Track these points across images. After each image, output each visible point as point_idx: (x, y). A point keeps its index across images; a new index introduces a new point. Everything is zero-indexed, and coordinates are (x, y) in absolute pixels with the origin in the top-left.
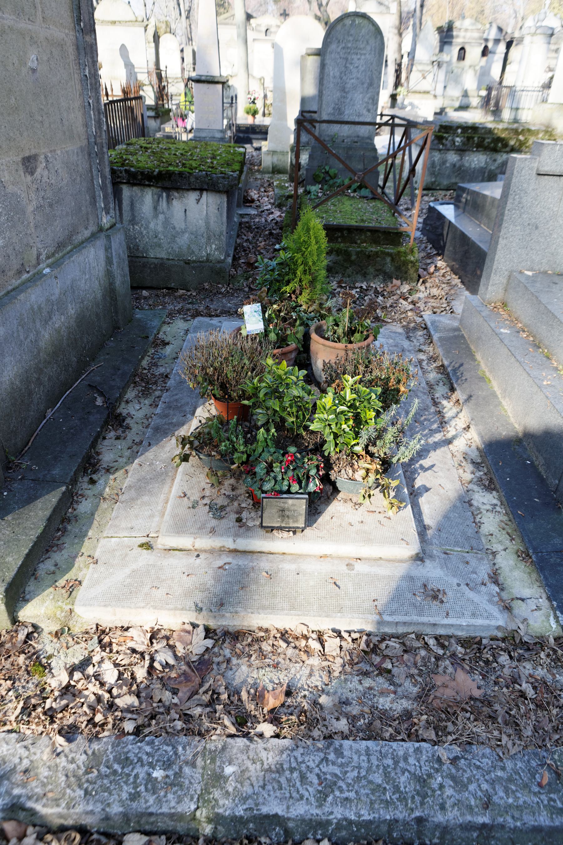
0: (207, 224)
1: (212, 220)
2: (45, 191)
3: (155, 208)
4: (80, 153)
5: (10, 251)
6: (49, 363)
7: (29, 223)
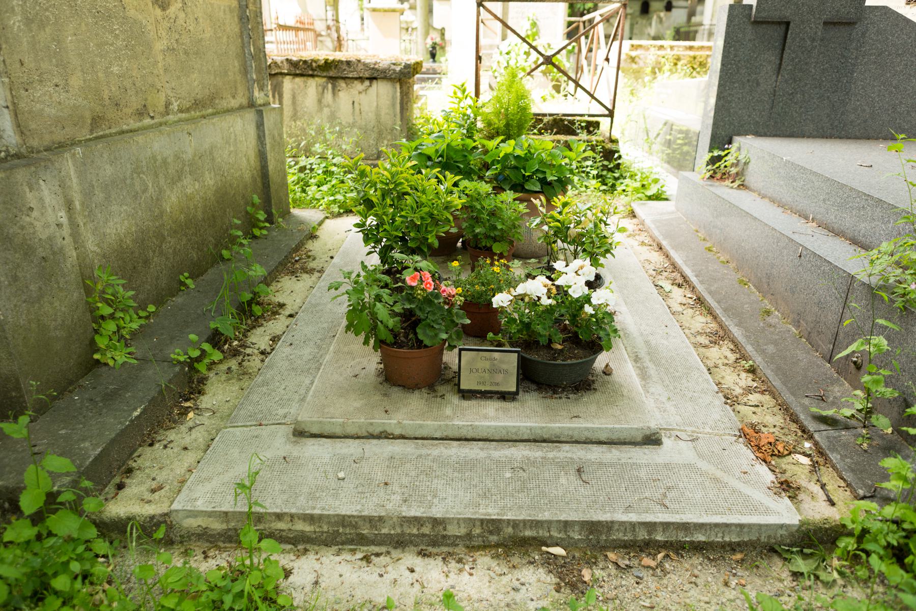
0: (378, 115)
1: (384, 111)
2: (180, 35)
3: (320, 101)
4: (228, 12)
5: (127, 83)
6: (175, 232)
7: (156, 62)
